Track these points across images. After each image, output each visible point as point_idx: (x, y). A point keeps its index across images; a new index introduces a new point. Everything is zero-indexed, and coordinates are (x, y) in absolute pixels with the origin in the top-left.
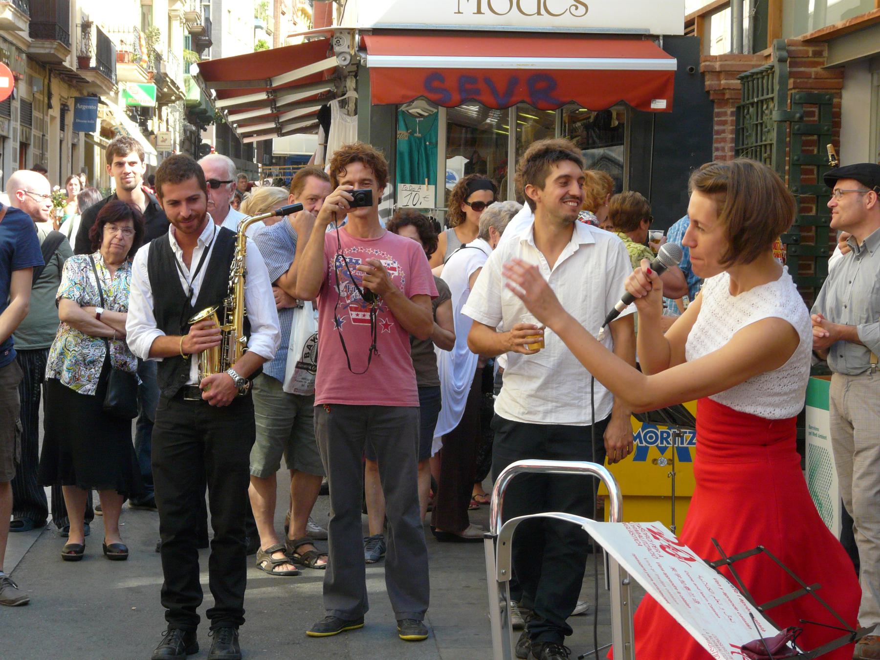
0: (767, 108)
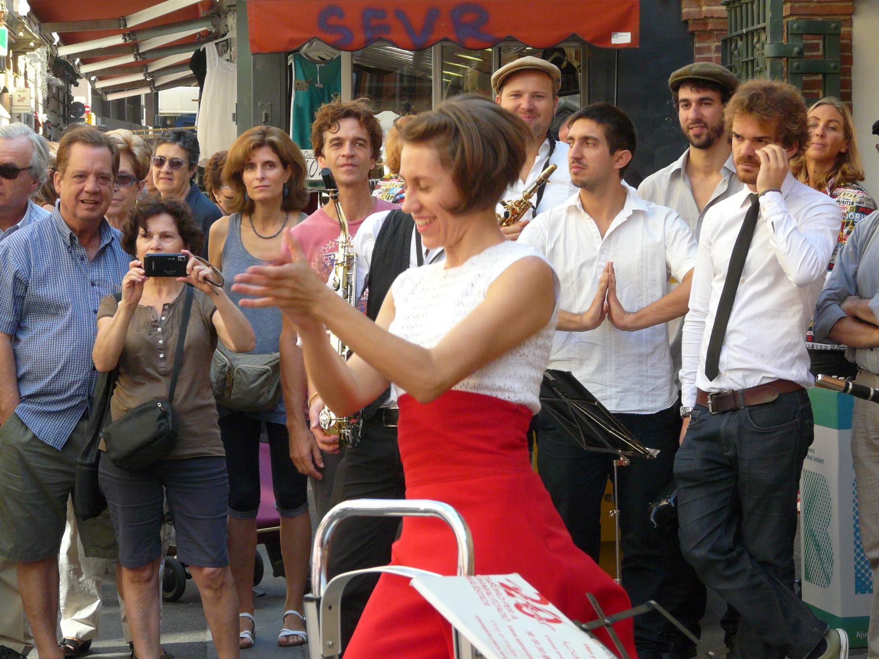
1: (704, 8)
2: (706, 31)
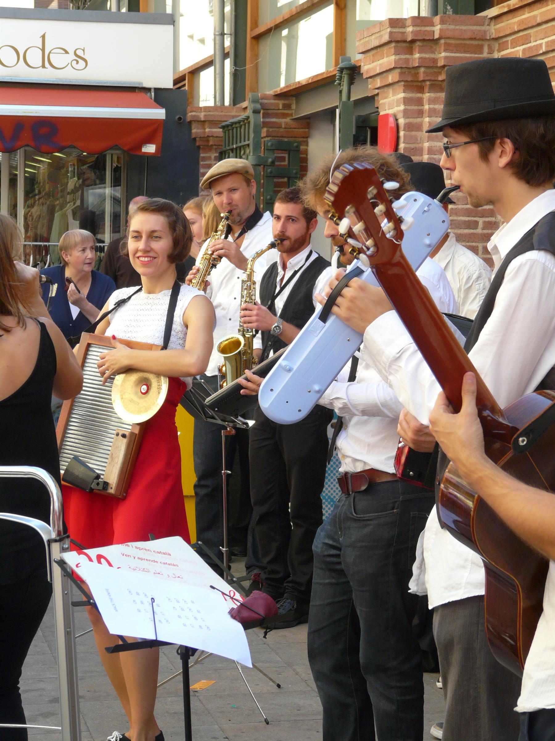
0: (244, 153)
1: (207, 130)
2: (208, 146)
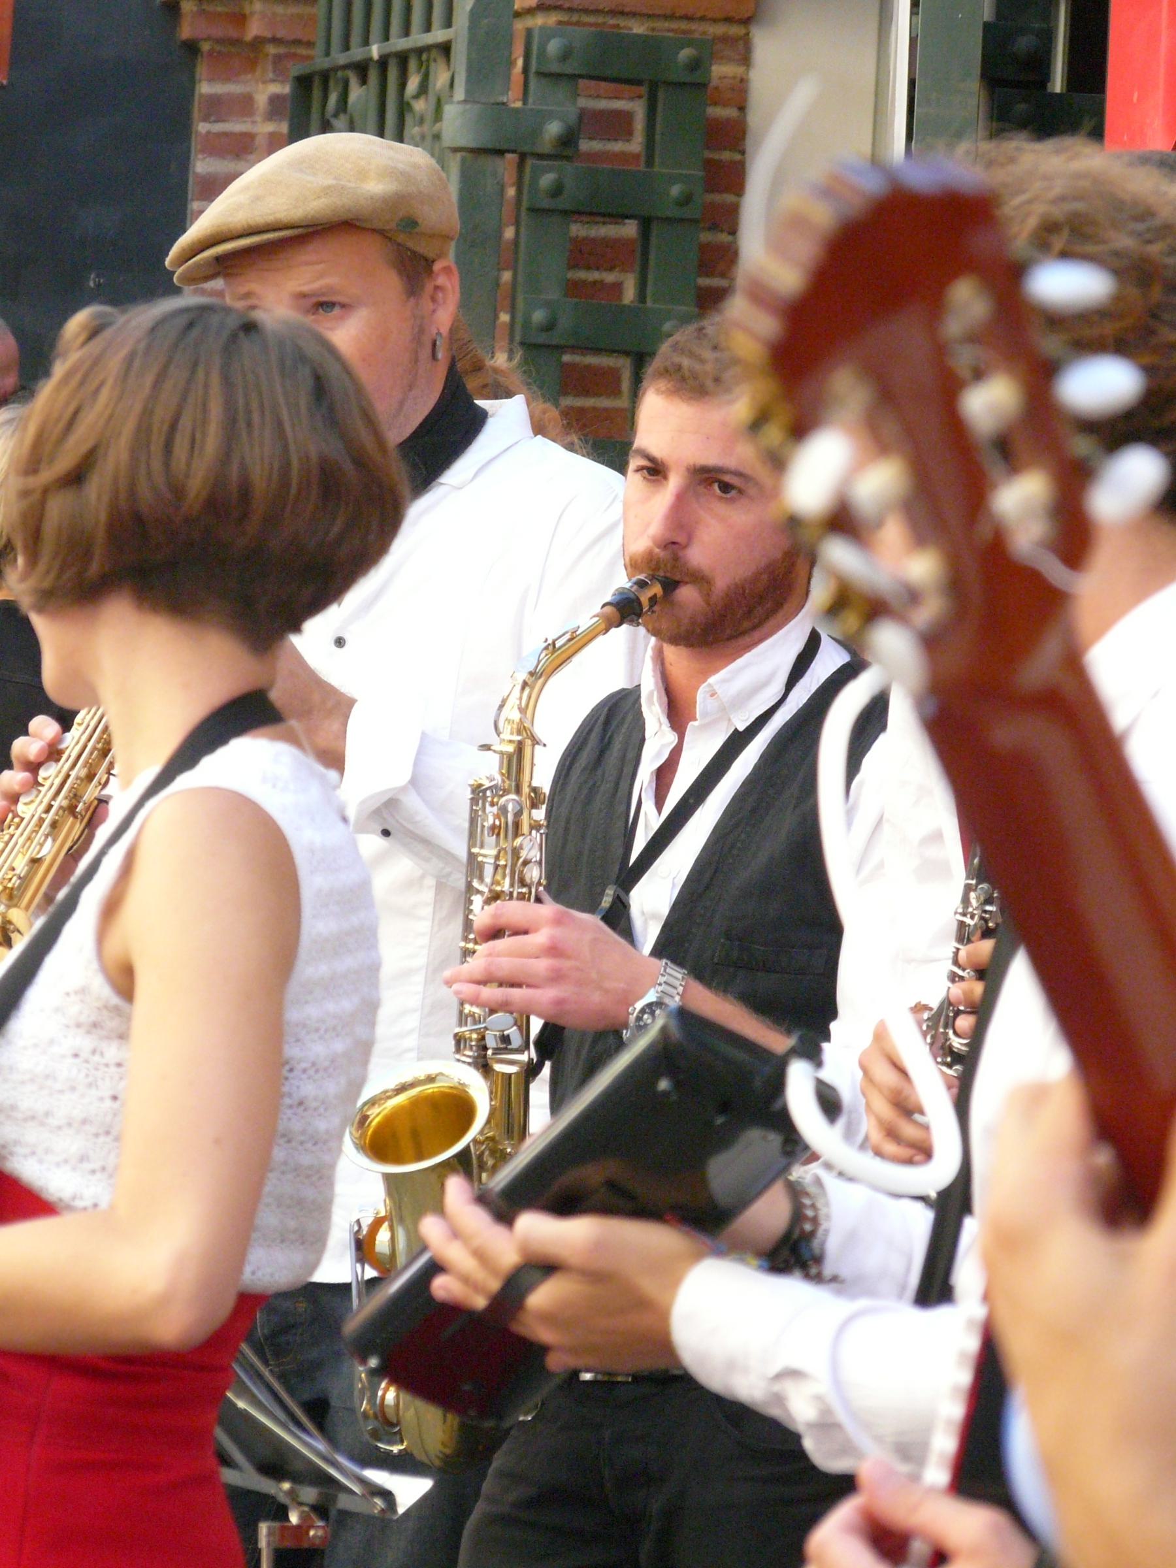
0: (423, 89)
2: (236, 42)
